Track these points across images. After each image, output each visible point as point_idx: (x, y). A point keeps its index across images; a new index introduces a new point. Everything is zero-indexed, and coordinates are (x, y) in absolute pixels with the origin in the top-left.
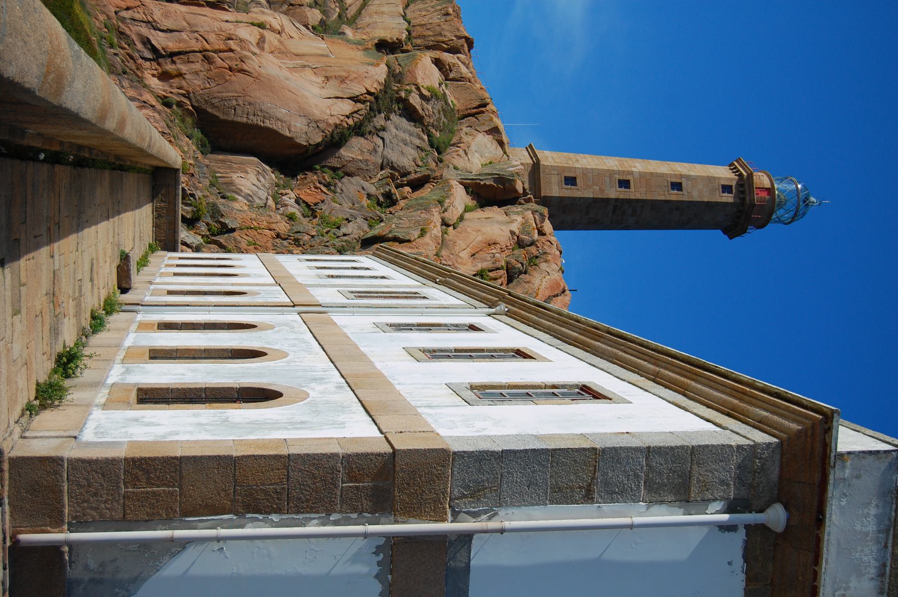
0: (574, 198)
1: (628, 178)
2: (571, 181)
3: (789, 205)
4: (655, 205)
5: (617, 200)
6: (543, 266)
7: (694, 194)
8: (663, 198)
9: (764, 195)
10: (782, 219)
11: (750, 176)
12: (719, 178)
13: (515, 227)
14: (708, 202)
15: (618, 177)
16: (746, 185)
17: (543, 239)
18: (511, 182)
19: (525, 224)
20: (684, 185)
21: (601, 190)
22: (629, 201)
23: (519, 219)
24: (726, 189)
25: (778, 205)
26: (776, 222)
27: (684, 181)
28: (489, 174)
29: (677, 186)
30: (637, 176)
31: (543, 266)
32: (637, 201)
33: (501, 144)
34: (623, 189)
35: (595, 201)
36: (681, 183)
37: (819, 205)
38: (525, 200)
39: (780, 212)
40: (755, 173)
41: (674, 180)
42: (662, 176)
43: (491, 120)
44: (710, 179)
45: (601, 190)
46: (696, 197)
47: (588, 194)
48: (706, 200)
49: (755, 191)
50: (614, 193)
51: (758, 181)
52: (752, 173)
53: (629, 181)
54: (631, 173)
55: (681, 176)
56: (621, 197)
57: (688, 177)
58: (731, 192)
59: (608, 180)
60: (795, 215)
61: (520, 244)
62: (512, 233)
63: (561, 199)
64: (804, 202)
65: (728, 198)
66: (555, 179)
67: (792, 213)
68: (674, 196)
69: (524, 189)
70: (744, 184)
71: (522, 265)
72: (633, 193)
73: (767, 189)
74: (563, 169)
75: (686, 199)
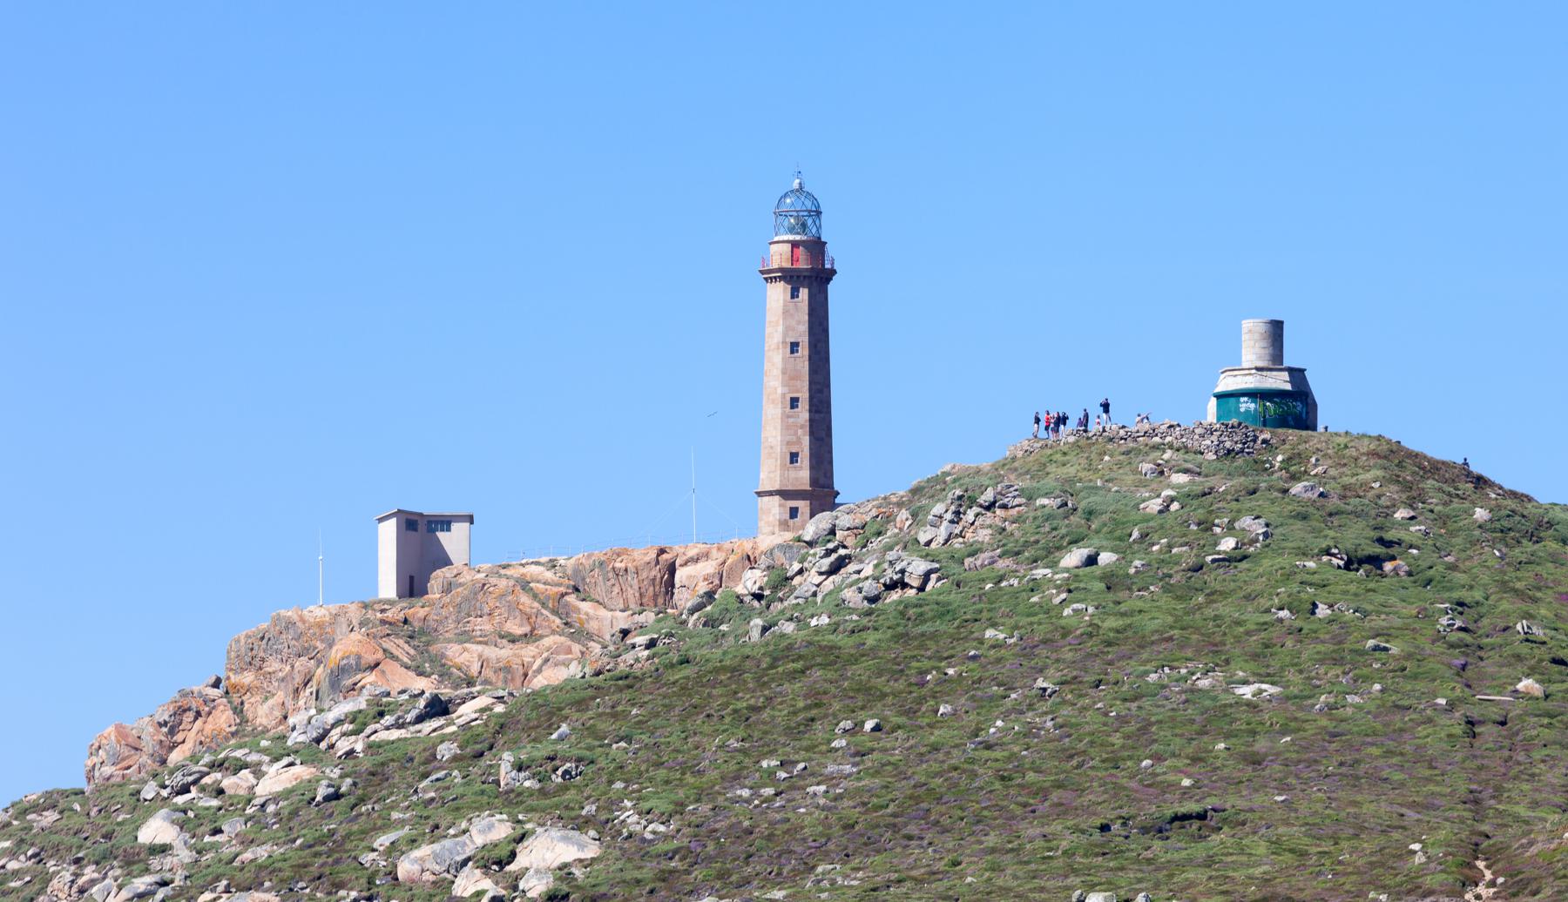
2: (794, 457)
15: (788, 409)
21: (802, 427)
29: (794, 347)
30: (786, 390)
32: (810, 390)
35: (812, 433)
44: (785, 312)
45: (802, 427)
46: (803, 328)
47: (806, 440)
50: (803, 413)
54: (784, 395)
57: (785, 335)
63: (812, 468)
65: (804, 293)
66: (792, 474)
68: (804, 351)
70: (791, 277)
74: (783, 466)
75: (806, 339)
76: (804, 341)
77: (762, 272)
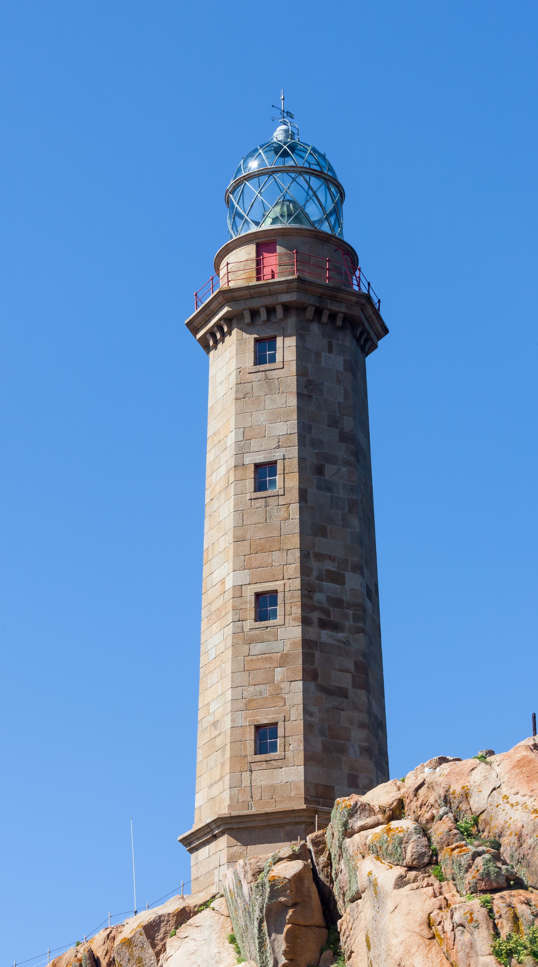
0: (308, 727)
1: (249, 594)
2: (265, 737)
3: (296, 192)
4: (314, 527)
5: (305, 621)
6: (477, 802)
7: (279, 431)
8: (295, 508)
9: (271, 261)
10: (330, 206)
11: (228, 296)
12: (239, 371)
13: (386, 874)
14: (300, 395)
16: (255, 303)
17: (412, 806)
18: (276, 888)
19: (377, 851)
20: (260, 458)
22: (307, 591)
23: (368, 866)
24: (263, 352)
25: (297, 220)
26: (338, 221)
27: (251, 459)
28: (262, 945)
29: (264, 473)
30: (244, 577)
31: (477, 802)
32: (305, 570)
33: (183, 916)
34: (280, 609)
35: (310, 675)
36: (258, 466)
37: (290, 115)
38: (319, 853)
39: (314, 212)
40: (223, 284)
41: (250, 484)
42: (240, 512)
43: (128, 943)
44: (243, 395)
46: (288, 426)
48: (293, 401)
49: (267, 279)
50: (288, 631)
51: (242, 275)
52: (222, 293)
53: (258, 595)
54: (239, 589)
55: (239, 466)
56: (297, 611)
58: (273, 339)
59: (258, 648)
60: (319, 175)
61: (426, 863)
62: (401, 882)
63: (310, 759)
64: (285, 154)
65: (287, 348)
66: (262, 778)
67: (315, 182)
68: (288, 482)
69: (293, 857)
70: (253, 312)
71: (479, 854)
72: (289, 584)
73: (259, 253)
75: (294, 452)
76: (288, 457)
77: (193, 327)
